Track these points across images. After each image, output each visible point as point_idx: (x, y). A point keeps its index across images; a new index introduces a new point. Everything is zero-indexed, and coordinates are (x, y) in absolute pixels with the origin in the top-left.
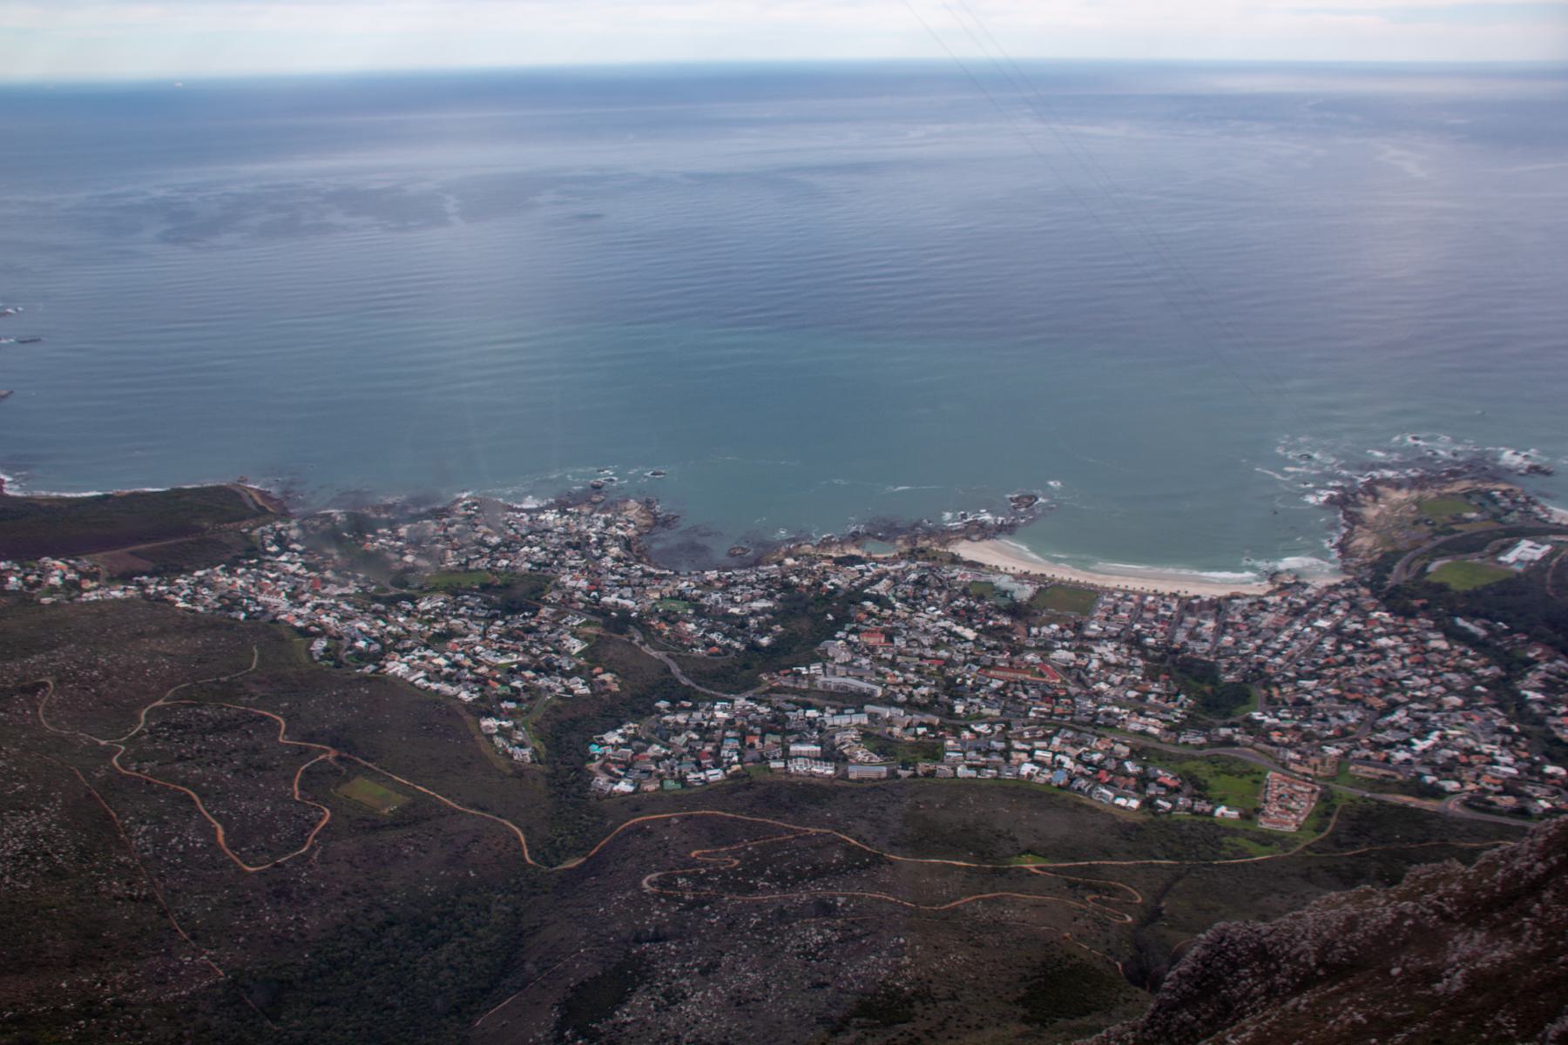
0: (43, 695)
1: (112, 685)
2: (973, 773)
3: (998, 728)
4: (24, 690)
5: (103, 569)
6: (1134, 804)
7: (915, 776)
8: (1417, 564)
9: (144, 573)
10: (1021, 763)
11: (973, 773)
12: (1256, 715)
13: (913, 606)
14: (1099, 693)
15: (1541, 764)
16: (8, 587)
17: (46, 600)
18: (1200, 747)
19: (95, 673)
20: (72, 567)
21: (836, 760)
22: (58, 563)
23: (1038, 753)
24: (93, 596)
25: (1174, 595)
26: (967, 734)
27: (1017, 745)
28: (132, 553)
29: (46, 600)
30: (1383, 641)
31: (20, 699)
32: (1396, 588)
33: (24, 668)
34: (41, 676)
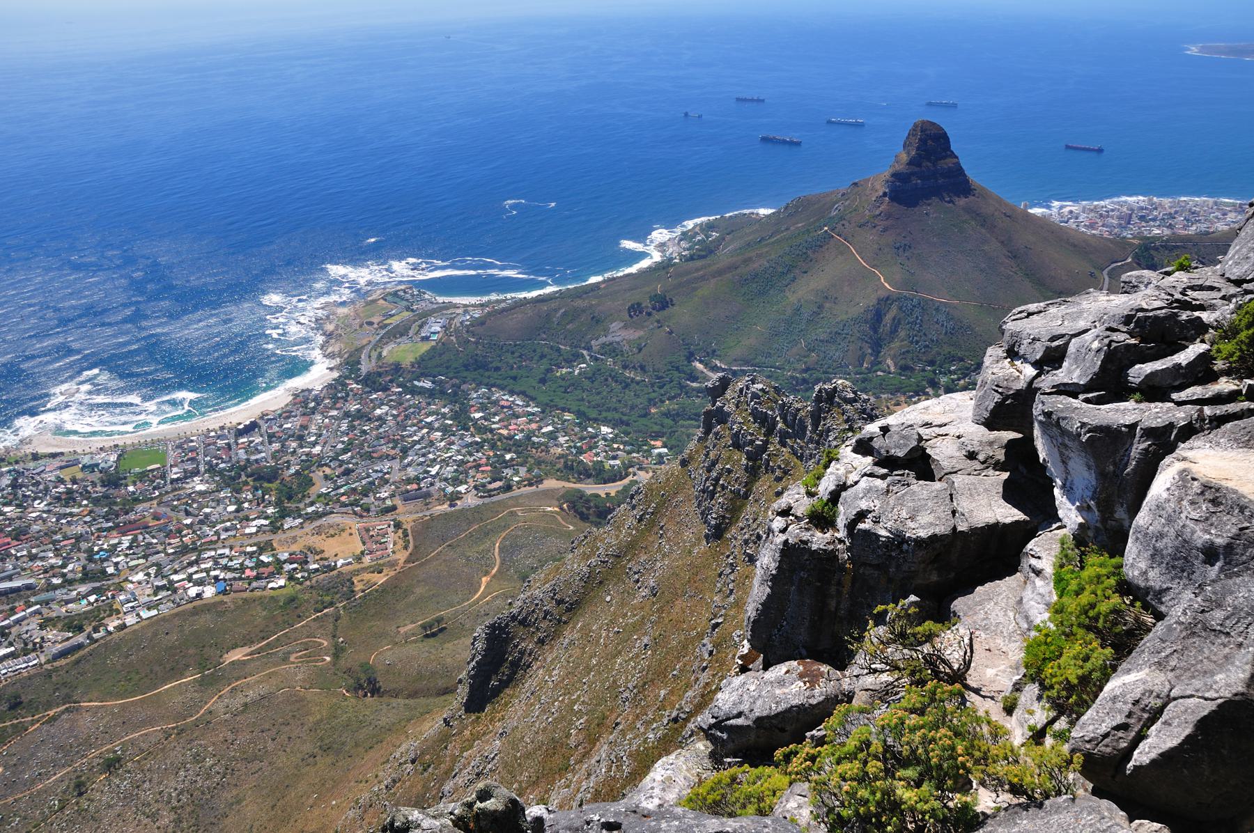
2: (154, 612)
3: (152, 571)
6: (282, 582)
7: (110, 633)
8: (374, 355)
10: (186, 589)
11: (154, 612)
12: (324, 490)
13: (18, 506)
14: (207, 516)
15: (503, 456)
18: (301, 526)
21: (34, 650)
23: (195, 577)
25: (222, 428)
26: (130, 586)
27: (175, 577)
30: (378, 412)
32: (369, 374)
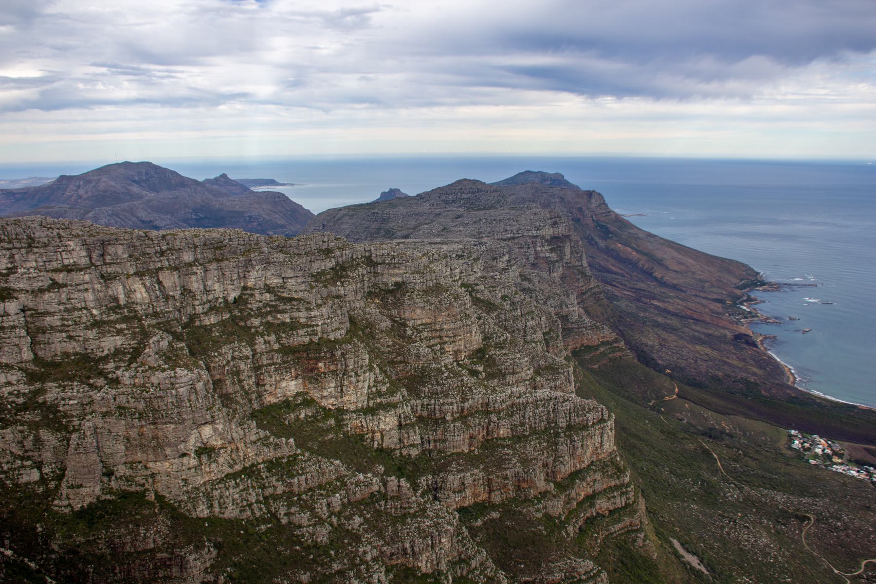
0: (807, 525)
1: (847, 536)
4: (797, 517)
5: (846, 453)
9: (871, 465)
16: (794, 446)
17: (812, 462)
19: (839, 524)
20: (829, 446)
22: (822, 441)
24: (839, 469)
28: (865, 449)
29: (812, 462)
31: (794, 522)
33: (799, 503)
34: (807, 512)
